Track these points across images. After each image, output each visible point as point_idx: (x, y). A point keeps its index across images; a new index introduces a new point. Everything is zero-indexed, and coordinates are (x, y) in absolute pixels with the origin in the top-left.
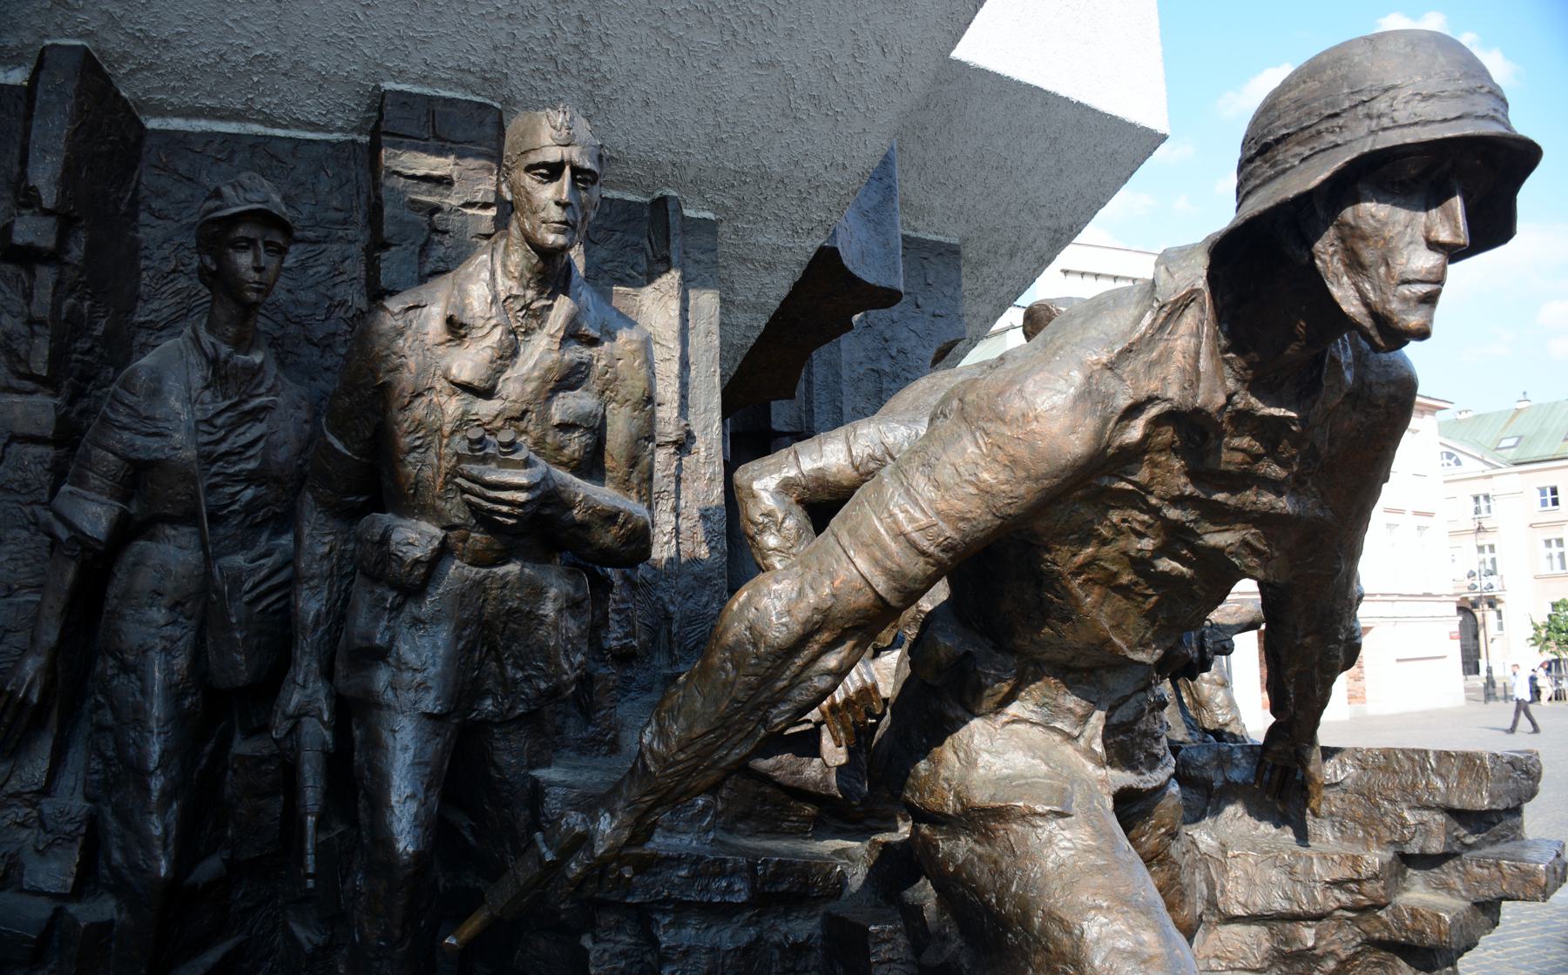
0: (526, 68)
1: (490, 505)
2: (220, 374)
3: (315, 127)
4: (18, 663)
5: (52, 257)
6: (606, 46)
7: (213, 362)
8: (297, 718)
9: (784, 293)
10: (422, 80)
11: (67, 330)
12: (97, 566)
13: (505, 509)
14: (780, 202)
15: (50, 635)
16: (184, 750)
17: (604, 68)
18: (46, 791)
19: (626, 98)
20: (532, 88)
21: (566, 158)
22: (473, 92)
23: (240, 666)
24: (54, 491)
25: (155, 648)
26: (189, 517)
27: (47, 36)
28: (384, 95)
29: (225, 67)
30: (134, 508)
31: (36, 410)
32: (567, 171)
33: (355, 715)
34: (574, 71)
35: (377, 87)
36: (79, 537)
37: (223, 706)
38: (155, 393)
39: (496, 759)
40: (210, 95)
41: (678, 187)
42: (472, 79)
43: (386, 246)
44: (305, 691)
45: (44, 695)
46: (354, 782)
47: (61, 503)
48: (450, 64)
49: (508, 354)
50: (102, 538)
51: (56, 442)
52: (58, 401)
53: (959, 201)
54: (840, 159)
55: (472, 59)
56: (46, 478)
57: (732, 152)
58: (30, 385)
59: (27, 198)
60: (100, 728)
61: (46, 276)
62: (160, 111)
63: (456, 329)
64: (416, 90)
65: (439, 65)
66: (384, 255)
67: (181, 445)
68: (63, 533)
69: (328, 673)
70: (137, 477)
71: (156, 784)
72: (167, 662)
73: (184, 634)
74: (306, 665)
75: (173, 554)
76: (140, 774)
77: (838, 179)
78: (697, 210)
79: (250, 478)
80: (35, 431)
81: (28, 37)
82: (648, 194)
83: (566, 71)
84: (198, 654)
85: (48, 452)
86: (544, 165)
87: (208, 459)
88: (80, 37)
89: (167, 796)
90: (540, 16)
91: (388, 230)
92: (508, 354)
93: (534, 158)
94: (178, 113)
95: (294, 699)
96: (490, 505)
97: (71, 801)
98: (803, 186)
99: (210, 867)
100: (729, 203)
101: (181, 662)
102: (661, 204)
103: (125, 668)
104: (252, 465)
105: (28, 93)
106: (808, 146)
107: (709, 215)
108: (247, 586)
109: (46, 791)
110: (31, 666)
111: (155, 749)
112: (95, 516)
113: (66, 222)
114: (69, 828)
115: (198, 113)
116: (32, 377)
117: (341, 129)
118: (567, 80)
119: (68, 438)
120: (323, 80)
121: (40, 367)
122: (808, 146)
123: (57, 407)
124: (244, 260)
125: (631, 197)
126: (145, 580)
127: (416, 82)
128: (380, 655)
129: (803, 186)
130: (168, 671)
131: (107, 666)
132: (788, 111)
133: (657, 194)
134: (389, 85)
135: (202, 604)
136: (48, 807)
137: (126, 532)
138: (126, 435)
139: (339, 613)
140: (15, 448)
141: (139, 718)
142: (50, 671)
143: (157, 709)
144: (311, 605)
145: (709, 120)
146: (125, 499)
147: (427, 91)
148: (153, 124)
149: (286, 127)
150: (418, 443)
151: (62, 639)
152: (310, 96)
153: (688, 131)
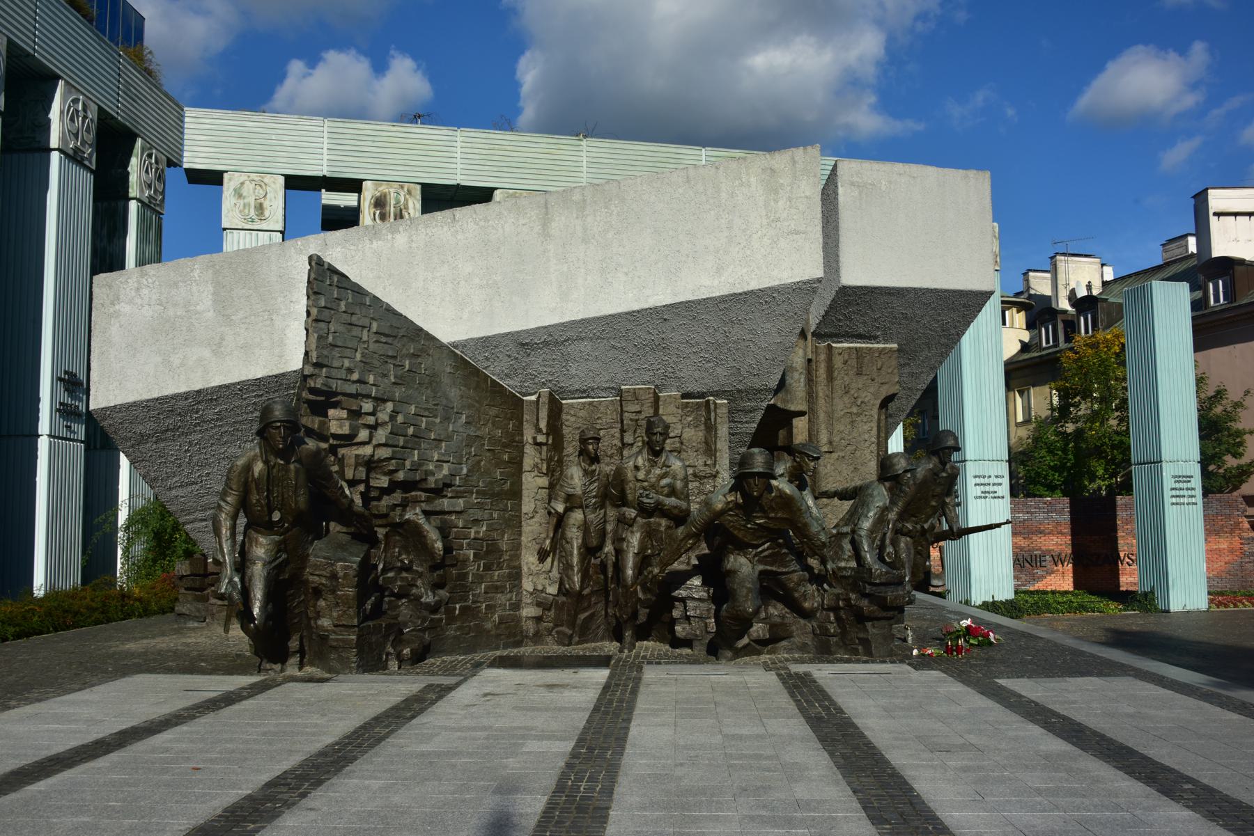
2: (586, 473)
5: (545, 444)
7: (585, 470)
11: (549, 460)
23: (594, 542)
25: (574, 536)
26: (581, 507)
31: (544, 481)
33: (619, 552)
36: (557, 512)
37: (589, 551)
38: (572, 478)
44: (609, 548)
46: (619, 567)
49: (648, 472)
59: (539, 431)
61: (545, 448)
63: (637, 468)
67: (578, 491)
69: (613, 543)
70: (569, 498)
73: (580, 534)
75: (577, 516)
76: (572, 567)
79: (594, 497)
84: (584, 539)
87: (584, 493)
92: (648, 472)
95: (606, 550)
97: (555, 574)
99: (586, 592)
110: (548, 542)
113: (548, 434)
119: (551, 487)
124: (591, 447)
126: (571, 521)
135: (585, 527)
137: (567, 510)
139: (615, 531)
141: (572, 555)
143: (575, 552)
144: (609, 528)
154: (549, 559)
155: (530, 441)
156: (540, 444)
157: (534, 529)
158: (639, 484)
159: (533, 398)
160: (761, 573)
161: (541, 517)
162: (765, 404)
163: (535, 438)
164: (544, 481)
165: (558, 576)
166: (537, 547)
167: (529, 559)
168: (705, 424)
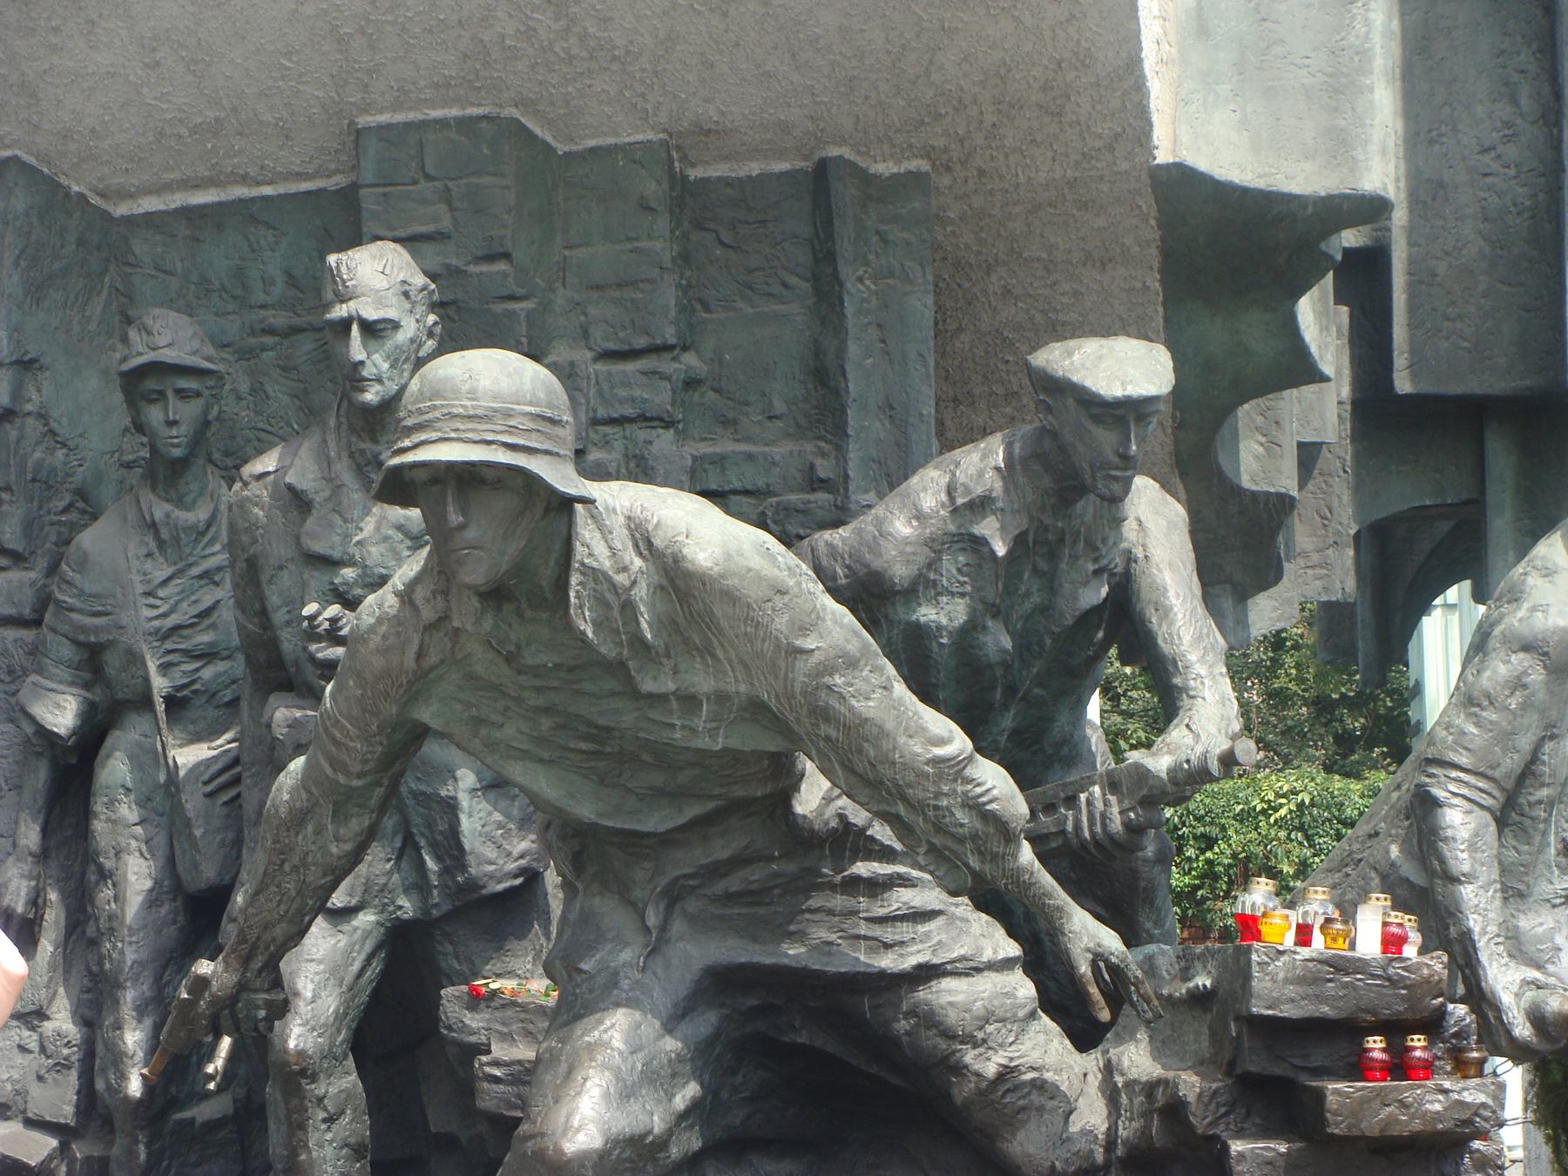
3: (307, 177)
6: (606, 20)
10: (397, 106)
17: (620, 42)
22: (472, 104)
28: (359, 133)
32: (355, 328)
34: (584, 54)
35: (352, 124)
36: (43, 733)
39: (443, 965)
41: (842, 141)
48: (422, 83)
50: (62, 731)
52: (32, 575)
64: (400, 117)
79: (208, 655)
82: (806, 158)
90: (500, 14)
94: (148, 191)
102: (823, 168)
104: (206, 638)
107: (922, 165)
108: (206, 777)
125: (784, 166)
133: (818, 155)
134: (364, 120)
146: (87, 686)
147: (412, 116)
148: (121, 210)
149: (271, 183)
160: (721, 983)
168: (816, 278)
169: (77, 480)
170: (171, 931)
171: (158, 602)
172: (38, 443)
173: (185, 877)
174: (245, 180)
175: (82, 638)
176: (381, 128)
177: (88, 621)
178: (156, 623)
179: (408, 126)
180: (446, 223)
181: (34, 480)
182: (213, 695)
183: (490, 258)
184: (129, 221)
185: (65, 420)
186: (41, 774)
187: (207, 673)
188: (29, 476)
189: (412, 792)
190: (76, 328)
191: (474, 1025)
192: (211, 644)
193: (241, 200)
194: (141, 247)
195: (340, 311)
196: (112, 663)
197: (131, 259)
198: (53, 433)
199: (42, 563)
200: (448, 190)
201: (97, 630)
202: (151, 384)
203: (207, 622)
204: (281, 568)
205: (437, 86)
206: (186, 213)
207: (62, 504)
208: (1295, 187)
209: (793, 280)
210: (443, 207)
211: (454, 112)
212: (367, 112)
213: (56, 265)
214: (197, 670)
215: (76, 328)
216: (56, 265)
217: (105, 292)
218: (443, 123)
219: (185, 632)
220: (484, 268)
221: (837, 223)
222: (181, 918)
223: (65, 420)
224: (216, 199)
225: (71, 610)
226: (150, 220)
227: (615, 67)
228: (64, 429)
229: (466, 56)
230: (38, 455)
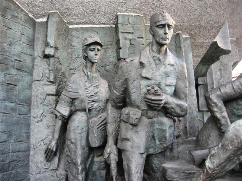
0: (148, 7)
1: (153, 105)
3: (104, 24)
4: (51, 142)
8: (109, 154)
9: (205, 53)
12: (66, 121)
13: (157, 105)
14: (204, 32)
15: (57, 136)
16: (84, 161)
17: (165, 5)
18: (57, 169)
19: (170, 11)
20: (150, 11)
21: (167, 23)
22: (137, 13)
24: (56, 106)
26: (84, 110)
27: (50, 11)
29: (85, 13)
30: (72, 108)
32: (167, 26)
34: (159, 6)
35: (117, 14)
36: (63, 116)
37: (92, 151)
39: (154, 162)
40: (82, 19)
42: (137, 10)
43: (121, 48)
44: (111, 149)
45: (57, 149)
47: (57, 108)
50: (67, 115)
51: (56, 95)
52: (55, 86)
53: (236, 30)
54: (218, 21)
55: (137, 6)
56: (54, 103)
57: (193, 22)
58: (50, 83)
59: (47, 45)
60: (68, 156)
61: (52, 60)
62: (72, 24)
63: (142, 64)
64: (125, 14)
65: (129, 8)
66: (120, 50)
68: (58, 115)
69: (116, 144)
71: (80, 168)
72: (81, 142)
74: (111, 141)
76: (76, 164)
77: (217, 25)
78: (186, 35)
80: (52, 93)
81: (46, 11)
83: (157, 6)
85: (54, 97)
86: (161, 25)
88: (56, 10)
89: (83, 170)
91: (121, 46)
93: (158, 24)
94: (76, 24)
95: (108, 149)
96: (153, 105)
98: (209, 28)
100: (193, 33)
101: (84, 142)
103: (72, 143)
104: (96, 98)
105: (47, 22)
106: (210, 19)
108: (97, 125)
109: (57, 169)
110: (54, 143)
111: (79, 161)
112: (64, 111)
114: (62, 177)
115: (80, 23)
116: (50, 82)
117: (109, 24)
118: (157, 8)
120: (105, 14)
121: (52, 79)
122: (210, 19)
123: (56, 88)
127: (125, 12)
128: (127, 139)
129: (209, 28)
130: (81, 144)
131: (68, 142)
132: (206, 11)
133: (177, 32)
136: (58, 172)
137: (72, 114)
138: (70, 93)
140: (48, 97)
142: (57, 144)
143: (79, 152)
144: (111, 128)
145: (188, 14)
146: (71, 107)
147: (127, 14)
148: (71, 27)
149: (98, 25)
150: (135, 91)
151: (59, 136)
152: (102, 17)
153: (184, 17)
154: (56, 159)
155: (41, 54)
156: (47, 57)
157: (42, 133)
158: (144, 83)
159: (44, 20)
161: (48, 120)
162: (211, 41)
163: (44, 51)
164: (52, 89)
165: (64, 173)
166: (44, 147)
167: (37, 158)
169: (63, 70)
170: (86, 154)
171: (88, 91)
172: (57, 63)
173: (91, 142)
174: (94, 24)
175: (71, 97)
176: (122, 15)
177: (73, 94)
178: (88, 95)
179: (126, 15)
180: (133, 31)
181: (56, 69)
182: (96, 109)
183: (140, 38)
184: (72, 29)
185: (61, 60)
186: (59, 123)
187: (95, 105)
188: (56, 68)
189: (157, 129)
190: (64, 44)
191: (175, 177)
192: (97, 99)
193: (92, 27)
194: (73, 33)
195: (163, 23)
196: (77, 103)
197: (72, 35)
198: (60, 61)
199: (57, 84)
200: (133, 26)
201: (75, 95)
202: (92, 47)
203: (96, 95)
204: (135, 80)
205: (134, 8)
206: (82, 28)
207: (60, 74)
208: (223, 48)
209: (173, 50)
210: (132, 29)
211: (134, 14)
212: (120, 12)
213: (62, 33)
214: (94, 104)
215: (64, 44)
216: (62, 33)
217: (68, 40)
218: (132, 16)
219: (92, 97)
220: (139, 39)
221: (181, 42)
222: (88, 151)
223: (61, 60)
224: (88, 27)
225: (70, 91)
226: (76, 29)
227: (161, 10)
228: (61, 62)
229: (141, 3)
230: (57, 65)
